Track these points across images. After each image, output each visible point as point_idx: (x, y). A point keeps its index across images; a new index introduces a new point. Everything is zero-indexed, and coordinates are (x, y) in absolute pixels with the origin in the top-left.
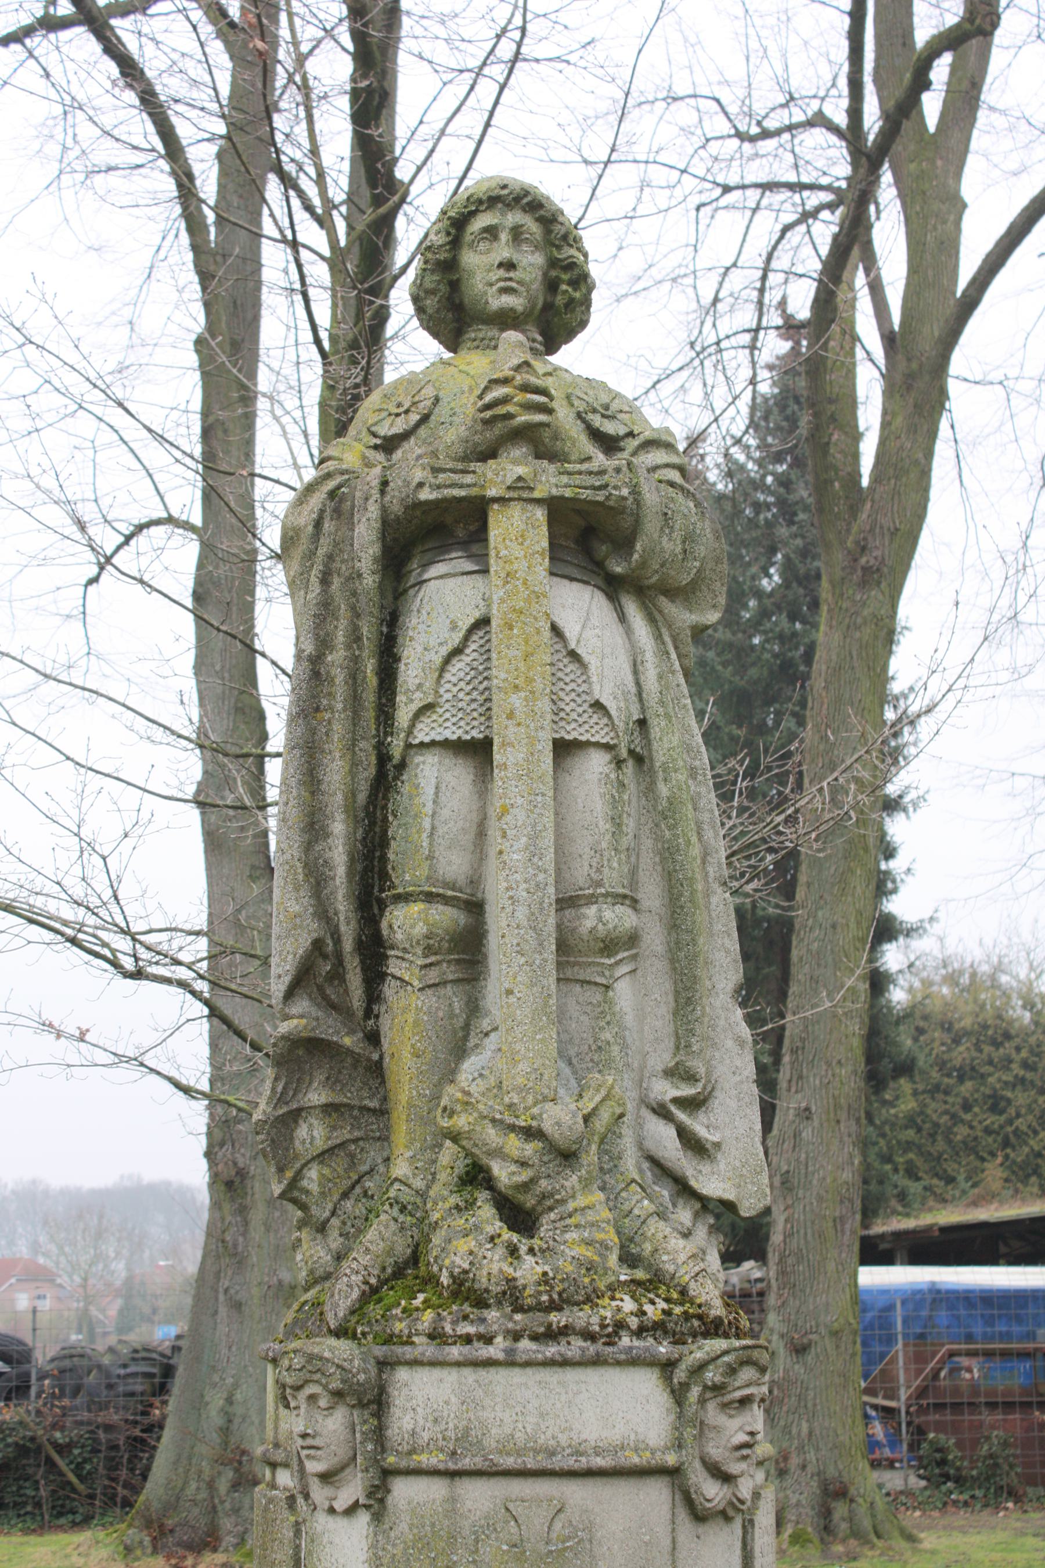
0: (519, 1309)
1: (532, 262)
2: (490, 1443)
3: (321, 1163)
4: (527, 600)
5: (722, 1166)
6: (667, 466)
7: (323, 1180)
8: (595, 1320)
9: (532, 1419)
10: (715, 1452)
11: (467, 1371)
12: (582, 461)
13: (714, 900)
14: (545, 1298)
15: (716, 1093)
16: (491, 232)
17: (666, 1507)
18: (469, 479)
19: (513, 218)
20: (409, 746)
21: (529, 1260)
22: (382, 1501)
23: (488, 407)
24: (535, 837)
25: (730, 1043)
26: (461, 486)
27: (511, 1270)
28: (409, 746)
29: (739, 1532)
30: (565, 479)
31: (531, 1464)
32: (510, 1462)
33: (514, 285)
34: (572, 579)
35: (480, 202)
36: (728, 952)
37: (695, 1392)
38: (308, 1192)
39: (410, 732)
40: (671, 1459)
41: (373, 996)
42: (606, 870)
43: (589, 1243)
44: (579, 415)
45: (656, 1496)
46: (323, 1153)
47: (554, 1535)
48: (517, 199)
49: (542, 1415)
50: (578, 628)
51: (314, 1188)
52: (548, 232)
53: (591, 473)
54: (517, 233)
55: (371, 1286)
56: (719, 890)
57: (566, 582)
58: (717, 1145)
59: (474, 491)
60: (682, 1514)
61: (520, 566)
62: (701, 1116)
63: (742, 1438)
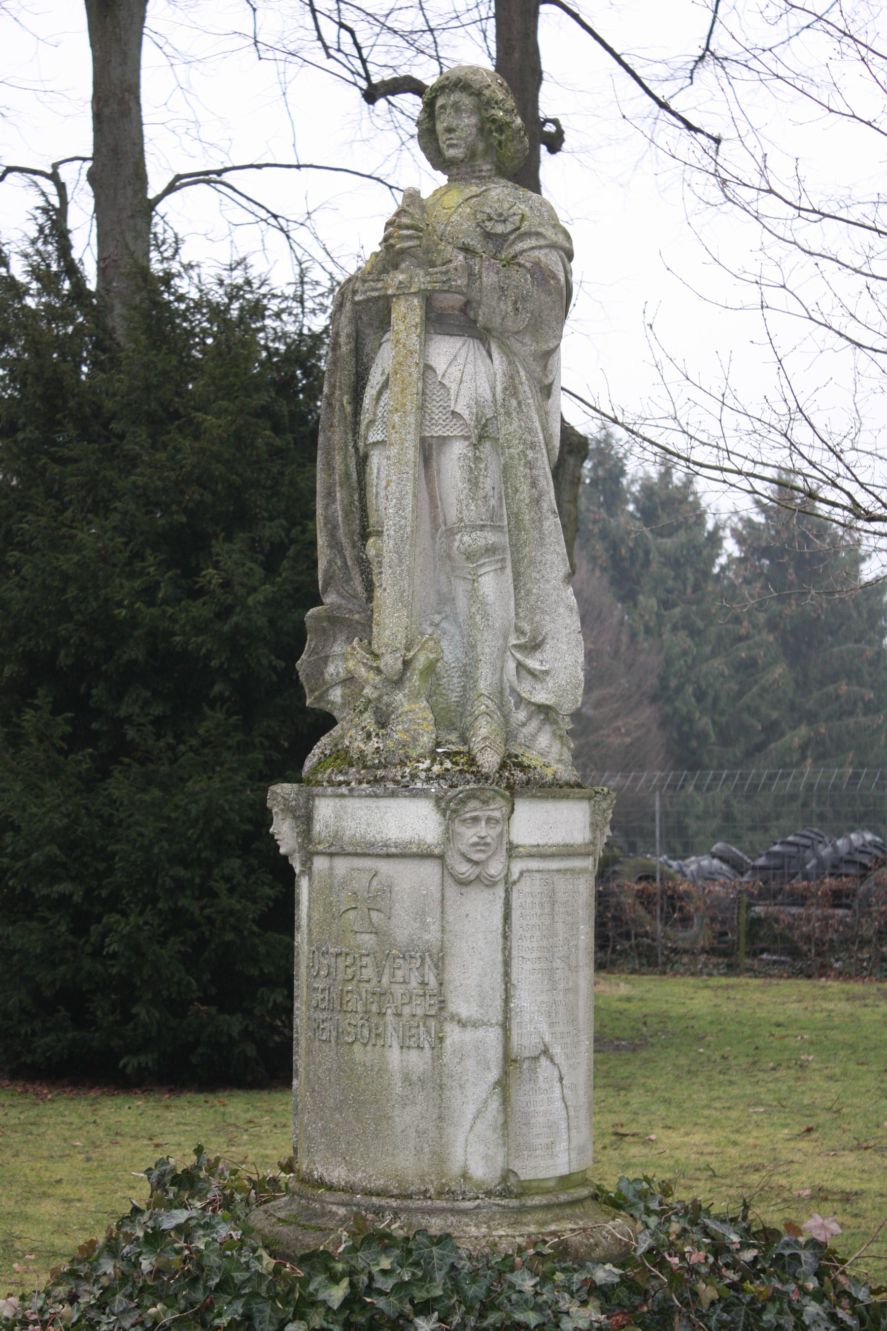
0: (365, 767)
2: (346, 839)
3: (345, 686)
4: (405, 357)
5: (550, 685)
6: (533, 248)
7: (343, 697)
8: (400, 773)
9: (363, 827)
10: (464, 848)
11: (337, 800)
12: (443, 264)
13: (546, 524)
14: (377, 761)
15: (548, 641)
17: (438, 877)
18: (380, 285)
19: (455, 97)
20: (366, 445)
21: (375, 740)
22: (310, 868)
24: (400, 499)
25: (561, 610)
26: (376, 290)
27: (362, 746)
28: (366, 445)
29: (503, 895)
30: (428, 278)
31: (359, 850)
32: (350, 849)
33: (455, 142)
34: (452, 335)
35: (436, 90)
36: (558, 554)
37: (448, 812)
38: (333, 703)
39: (366, 439)
40: (437, 851)
42: (465, 512)
43: (407, 731)
44: (478, 225)
45: (430, 871)
46: (345, 681)
47: (372, 888)
48: (456, 85)
49: (368, 825)
50: (444, 367)
51: (339, 700)
53: (442, 273)
55: (325, 755)
56: (551, 517)
57: (447, 337)
58: (546, 673)
59: (382, 293)
60: (449, 881)
61: (403, 336)
62: (538, 655)
63: (475, 839)
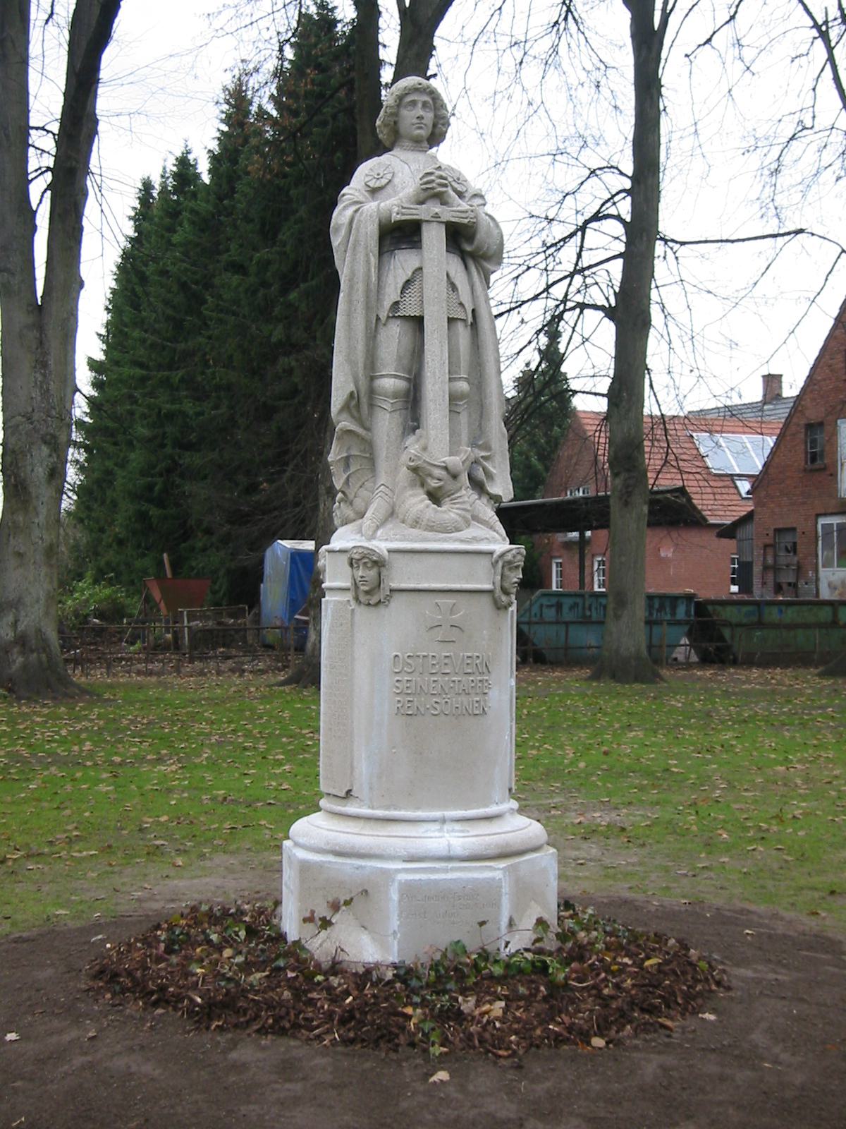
1: (429, 116)
16: (414, 103)
23: (426, 183)
37: (500, 564)
41: (371, 414)
52: (435, 103)
54: (425, 104)
